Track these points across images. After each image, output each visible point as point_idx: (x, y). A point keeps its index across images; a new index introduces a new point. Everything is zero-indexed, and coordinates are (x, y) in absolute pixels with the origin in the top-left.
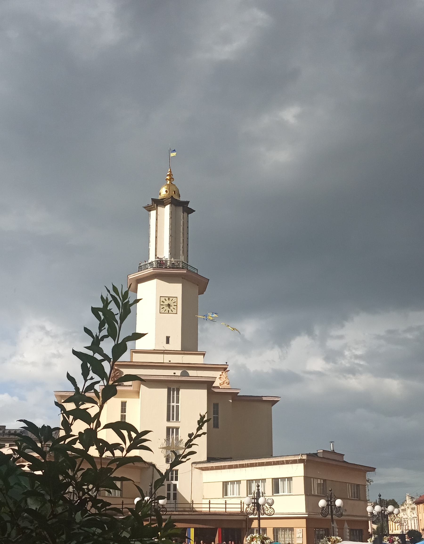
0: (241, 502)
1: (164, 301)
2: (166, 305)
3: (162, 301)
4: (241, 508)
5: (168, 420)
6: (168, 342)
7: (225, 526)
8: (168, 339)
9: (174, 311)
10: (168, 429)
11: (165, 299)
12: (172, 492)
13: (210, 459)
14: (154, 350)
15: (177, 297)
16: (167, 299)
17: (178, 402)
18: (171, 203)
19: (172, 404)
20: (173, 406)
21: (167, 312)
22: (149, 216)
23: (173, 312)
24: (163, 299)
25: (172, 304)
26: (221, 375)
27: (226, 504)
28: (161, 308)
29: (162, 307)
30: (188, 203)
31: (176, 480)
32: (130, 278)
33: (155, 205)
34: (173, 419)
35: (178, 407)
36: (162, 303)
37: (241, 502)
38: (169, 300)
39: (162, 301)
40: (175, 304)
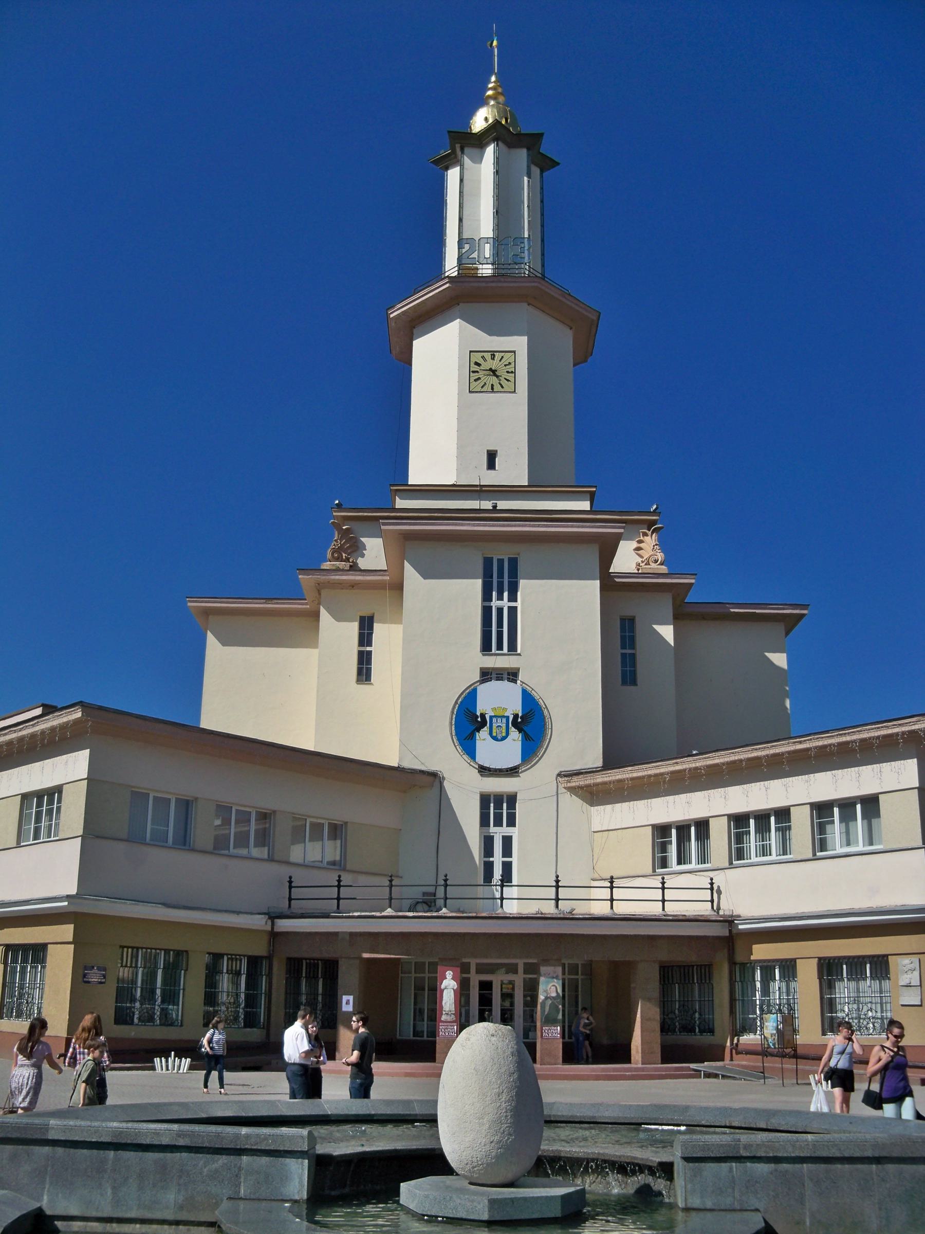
0: (712, 884)
1: (480, 361)
3: (477, 364)
4: (712, 901)
5: (486, 647)
6: (491, 465)
7: (665, 955)
8: (492, 457)
9: (508, 386)
11: (483, 357)
12: (498, 859)
13: (614, 757)
14: (454, 485)
15: (514, 352)
16: (488, 356)
17: (513, 598)
18: (496, 140)
19: (495, 603)
20: (500, 611)
23: (506, 389)
24: (477, 357)
25: (502, 372)
27: (663, 888)
28: (472, 380)
29: (476, 376)
31: (512, 823)
32: (392, 316)
33: (458, 146)
34: (500, 647)
35: (513, 611)
37: (712, 884)
38: (493, 359)
39: (477, 364)
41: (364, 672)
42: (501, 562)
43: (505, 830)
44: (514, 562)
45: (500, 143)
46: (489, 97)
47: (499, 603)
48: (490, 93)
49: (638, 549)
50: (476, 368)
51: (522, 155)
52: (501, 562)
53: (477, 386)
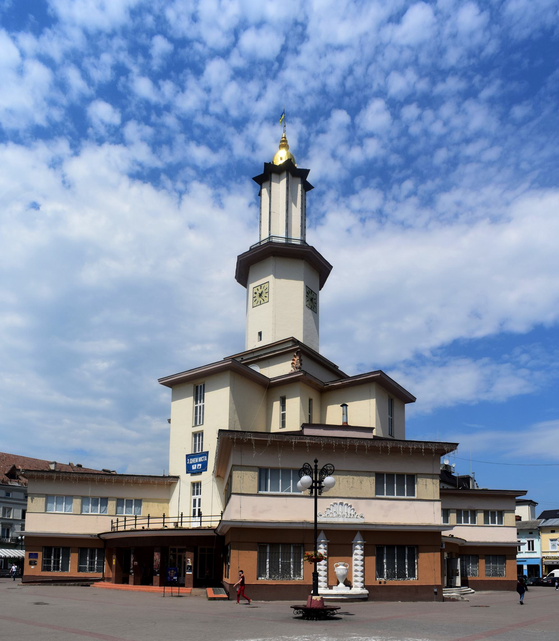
1: (256, 291)
12: (197, 508)
21: (259, 303)
36: (255, 295)
39: (256, 293)
40: (267, 291)
50: (255, 295)
53: (255, 304)
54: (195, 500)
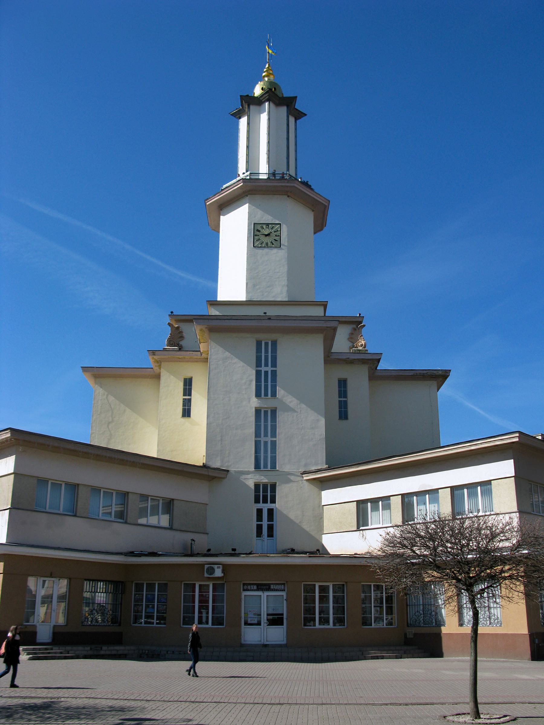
2: (262, 236)
10: (258, 411)
12: (265, 523)
17: (274, 364)
18: (268, 100)
20: (266, 373)
22: (238, 125)
26: (352, 334)
30: (293, 99)
31: (273, 501)
32: (207, 204)
34: (266, 395)
35: (274, 373)
41: (187, 413)
42: (266, 344)
43: (269, 505)
44: (274, 343)
45: (271, 103)
46: (264, 76)
47: (266, 369)
48: (264, 74)
49: (351, 338)
51: (284, 109)
52: (266, 344)
54: (259, 512)
